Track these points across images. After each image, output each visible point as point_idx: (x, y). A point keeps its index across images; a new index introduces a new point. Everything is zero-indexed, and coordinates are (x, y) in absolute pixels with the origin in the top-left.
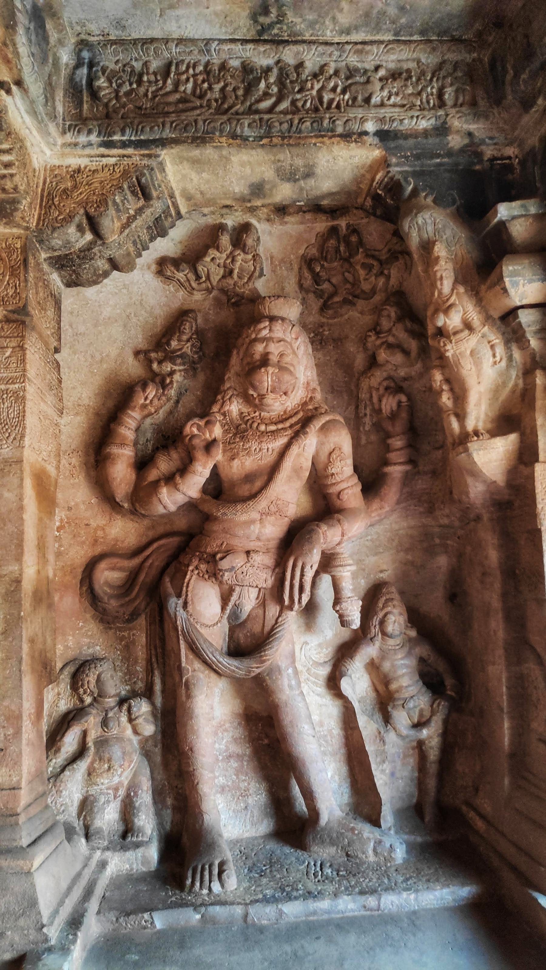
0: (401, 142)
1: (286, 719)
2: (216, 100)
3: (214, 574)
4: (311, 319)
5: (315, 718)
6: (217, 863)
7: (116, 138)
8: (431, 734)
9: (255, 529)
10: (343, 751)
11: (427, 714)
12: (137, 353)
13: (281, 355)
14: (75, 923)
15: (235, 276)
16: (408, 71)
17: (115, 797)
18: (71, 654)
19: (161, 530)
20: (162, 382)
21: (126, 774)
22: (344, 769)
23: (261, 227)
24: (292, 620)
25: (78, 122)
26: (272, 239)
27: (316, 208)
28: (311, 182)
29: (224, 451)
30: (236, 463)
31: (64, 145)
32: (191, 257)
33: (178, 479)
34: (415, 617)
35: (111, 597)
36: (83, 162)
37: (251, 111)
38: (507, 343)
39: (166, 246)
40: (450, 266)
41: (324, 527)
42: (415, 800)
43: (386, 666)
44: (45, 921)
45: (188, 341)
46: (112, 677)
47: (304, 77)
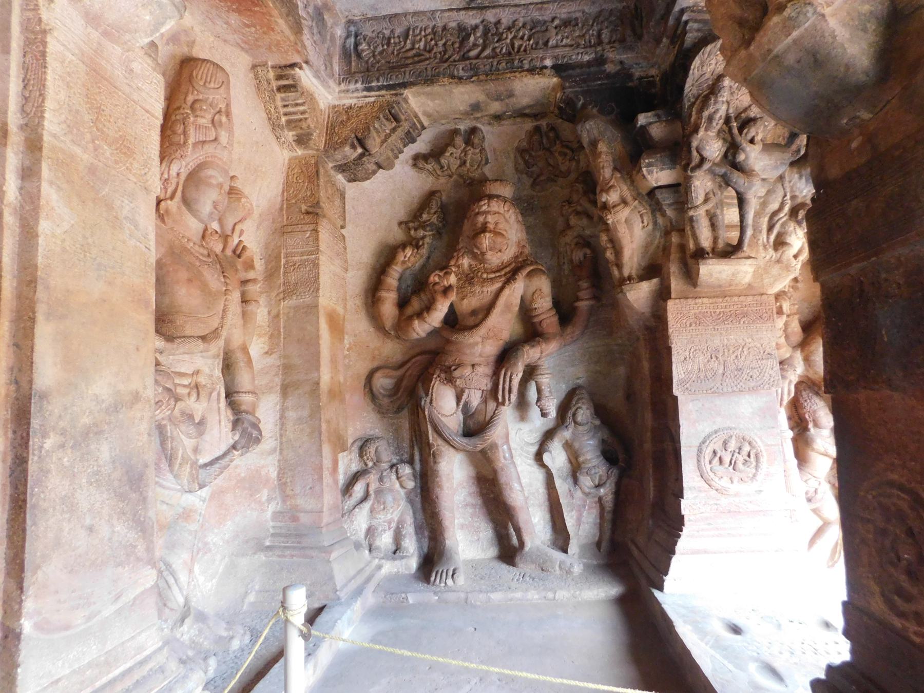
0: (571, 72)
1: (503, 479)
2: (440, 53)
3: (450, 380)
4: (525, 193)
5: (524, 481)
6: (452, 569)
7: (373, 84)
9: (478, 349)
10: (547, 503)
11: (604, 478)
13: (496, 224)
14: (359, 592)
15: (468, 165)
16: (576, 19)
17: (389, 528)
18: (359, 434)
19: (417, 350)
20: (416, 244)
21: (395, 513)
22: (548, 516)
23: (484, 128)
24: (507, 413)
25: (348, 76)
26: (493, 137)
27: (520, 114)
28: (514, 100)
29: (457, 294)
31: (340, 92)
32: (435, 154)
33: (425, 314)
34: (600, 411)
35: (384, 396)
36: (353, 102)
37: (464, 58)
38: (653, 212)
39: (421, 145)
40: (610, 158)
41: (527, 348)
42: (597, 538)
43: (576, 445)
45: (435, 213)
46: (386, 450)
47: (501, 30)
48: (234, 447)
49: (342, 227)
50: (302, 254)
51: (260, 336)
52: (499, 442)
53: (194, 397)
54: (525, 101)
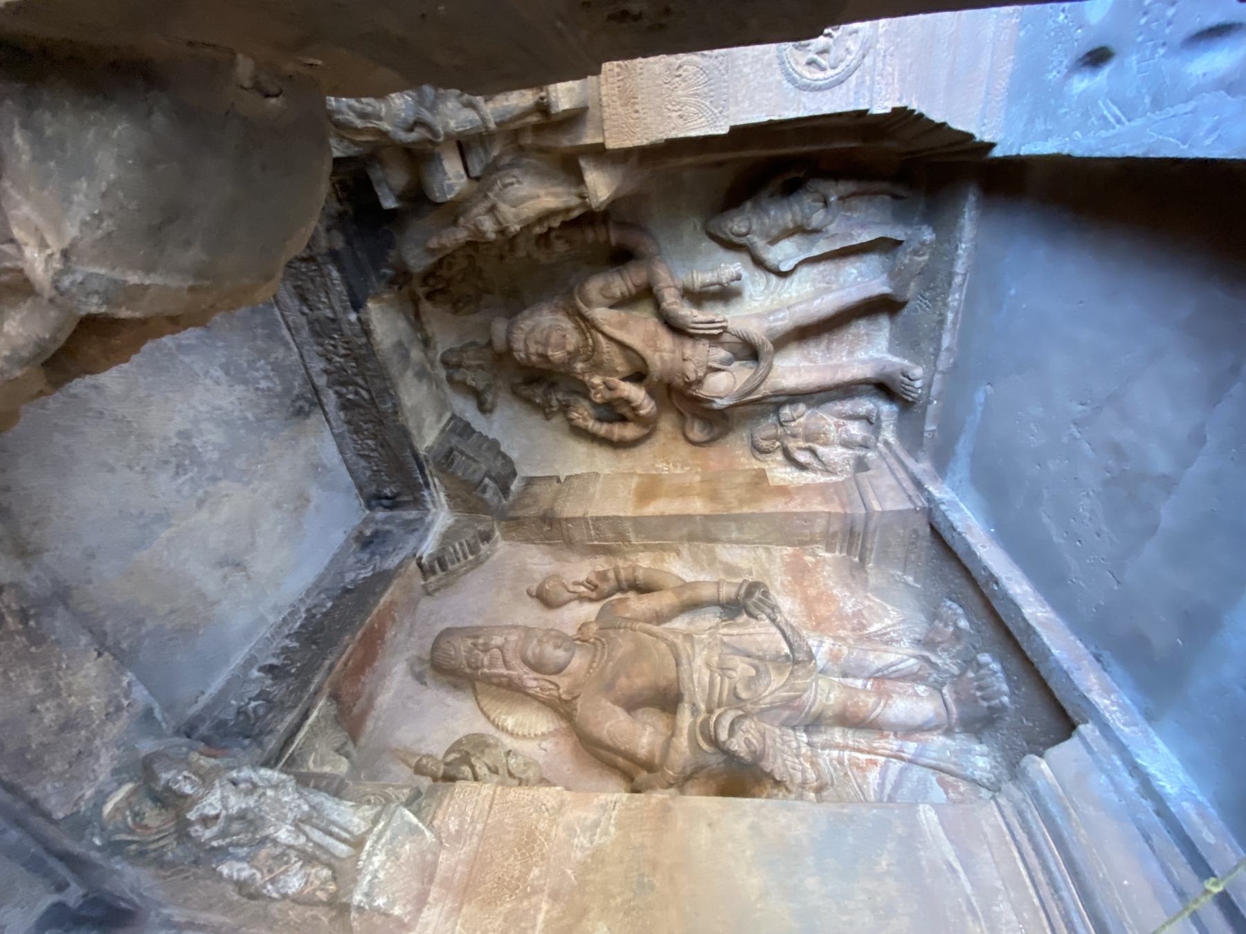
3: (699, 382)
8: (834, 191)
9: (666, 356)
11: (817, 196)
12: (548, 419)
18: (748, 452)
22: (852, 259)
23: (440, 350)
25: (418, 503)
27: (416, 320)
30: (619, 369)
31: (435, 506)
33: (634, 405)
36: (442, 495)
41: (664, 305)
43: (775, 232)
44: (912, 507)
47: (333, 369)
48: (773, 621)
49: (559, 481)
50: (588, 528)
51: (663, 560)
52: (766, 325)
53: (734, 674)
54: (402, 324)
